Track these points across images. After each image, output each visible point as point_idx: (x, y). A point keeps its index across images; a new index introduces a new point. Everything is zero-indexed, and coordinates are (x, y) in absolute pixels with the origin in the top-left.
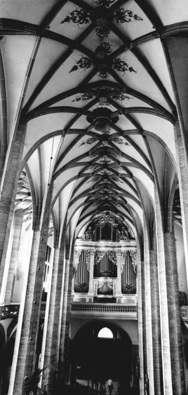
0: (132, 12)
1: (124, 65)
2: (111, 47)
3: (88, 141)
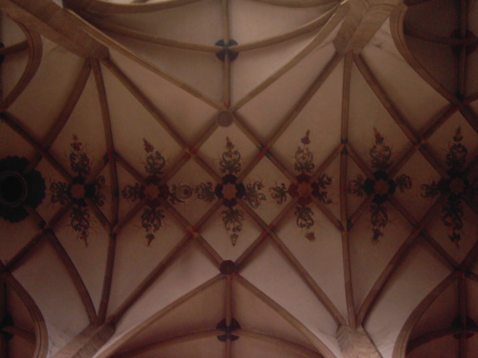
1: (155, 226)
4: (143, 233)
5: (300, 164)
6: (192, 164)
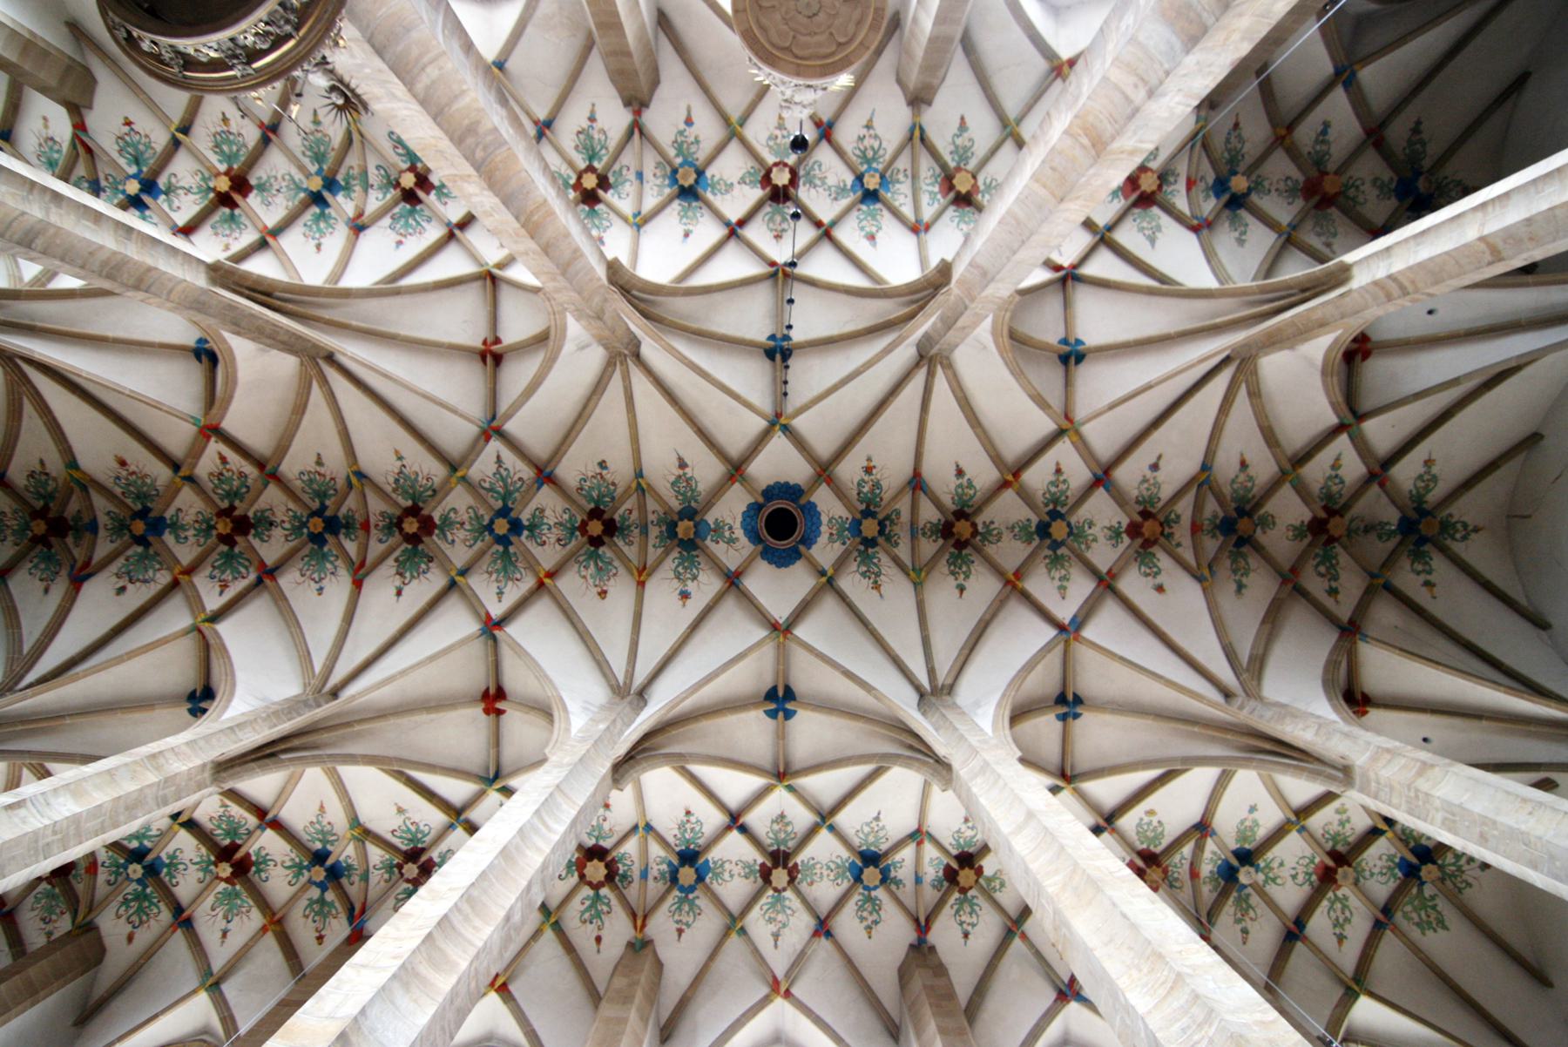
3: (688, 481)
4: (951, 582)
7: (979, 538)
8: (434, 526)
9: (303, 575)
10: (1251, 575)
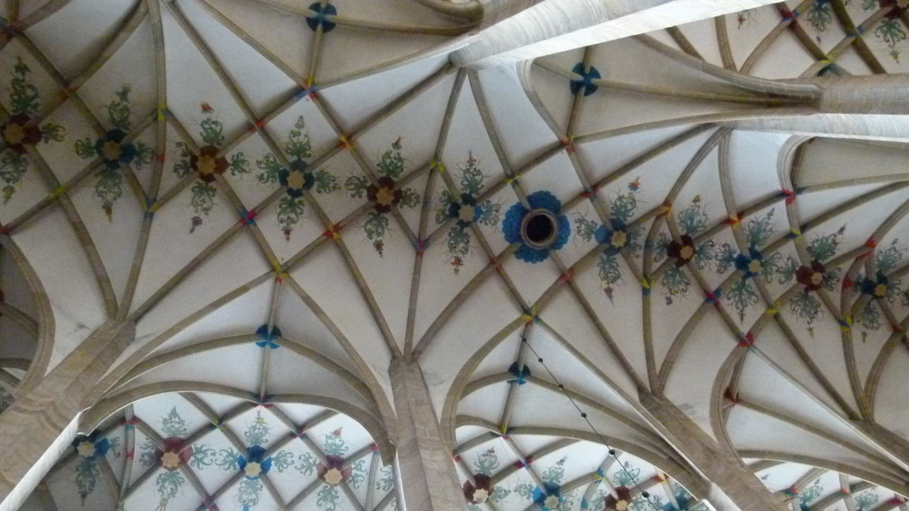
0: (291, 130)
1: (390, 157)
2: (355, 175)
3: (606, 278)
4: (403, 153)
5: (209, 195)
6: (335, 218)
7: (368, 184)
8: (798, 273)
9: (901, 255)
10: (109, 103)
